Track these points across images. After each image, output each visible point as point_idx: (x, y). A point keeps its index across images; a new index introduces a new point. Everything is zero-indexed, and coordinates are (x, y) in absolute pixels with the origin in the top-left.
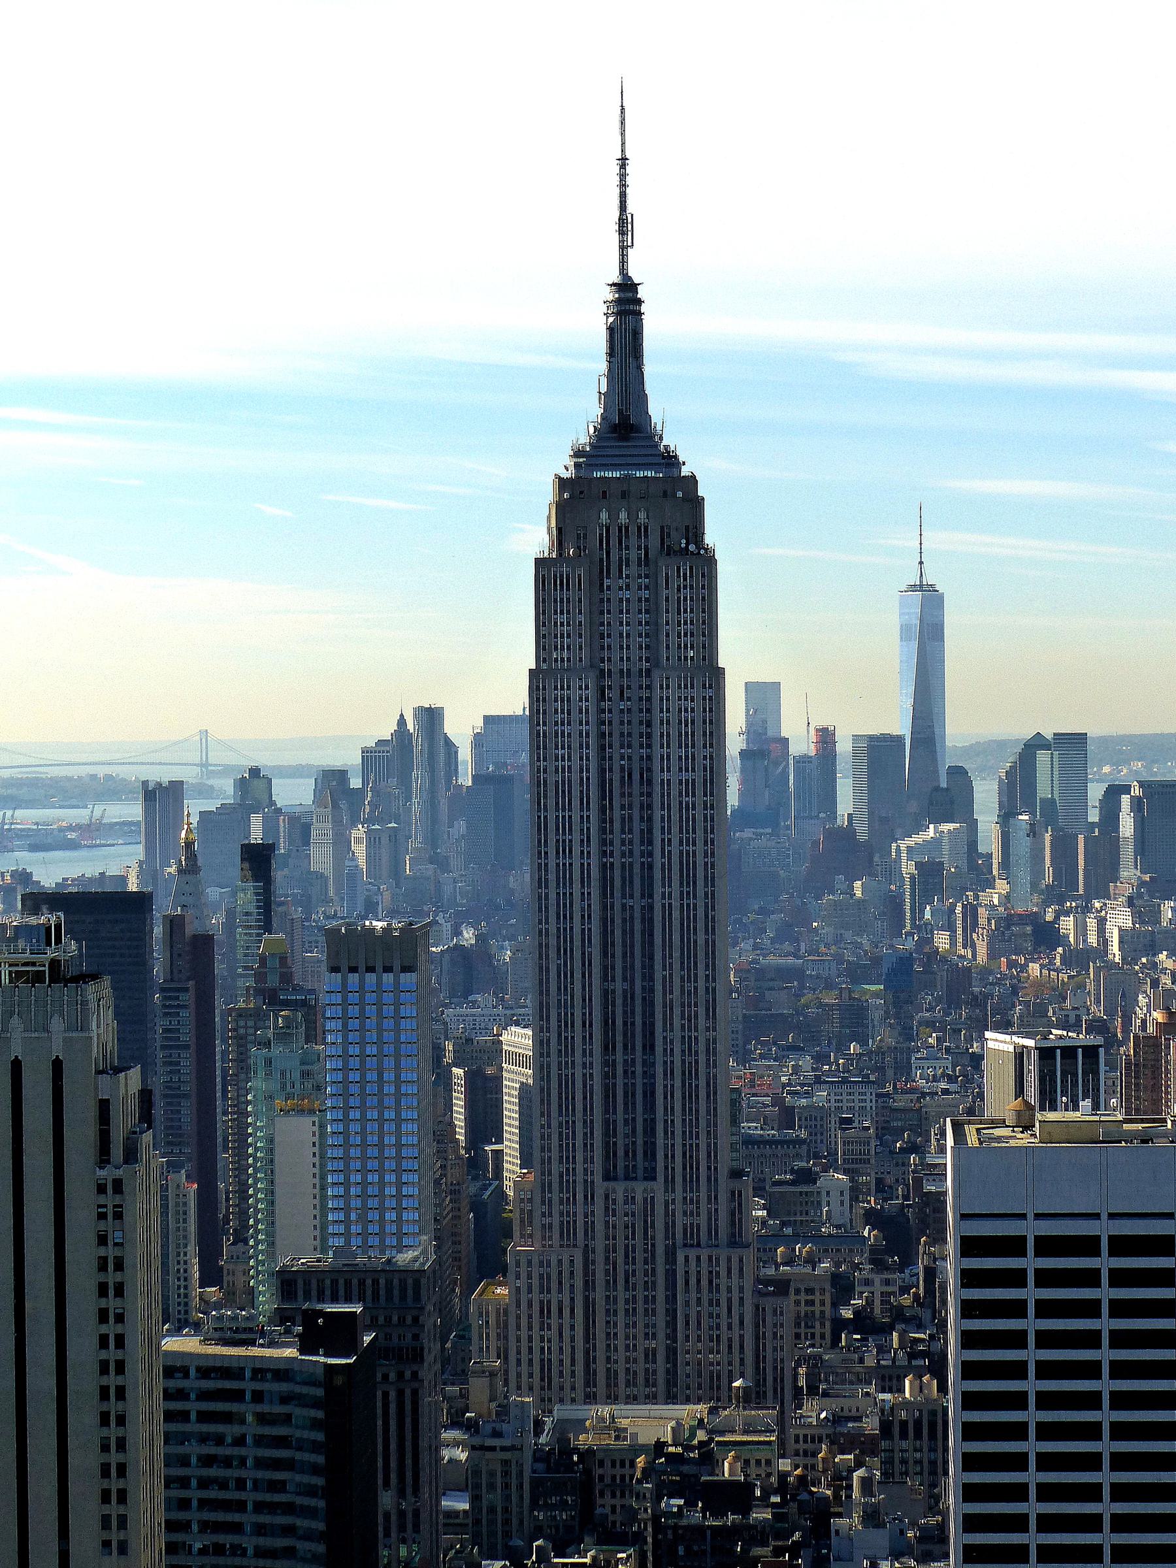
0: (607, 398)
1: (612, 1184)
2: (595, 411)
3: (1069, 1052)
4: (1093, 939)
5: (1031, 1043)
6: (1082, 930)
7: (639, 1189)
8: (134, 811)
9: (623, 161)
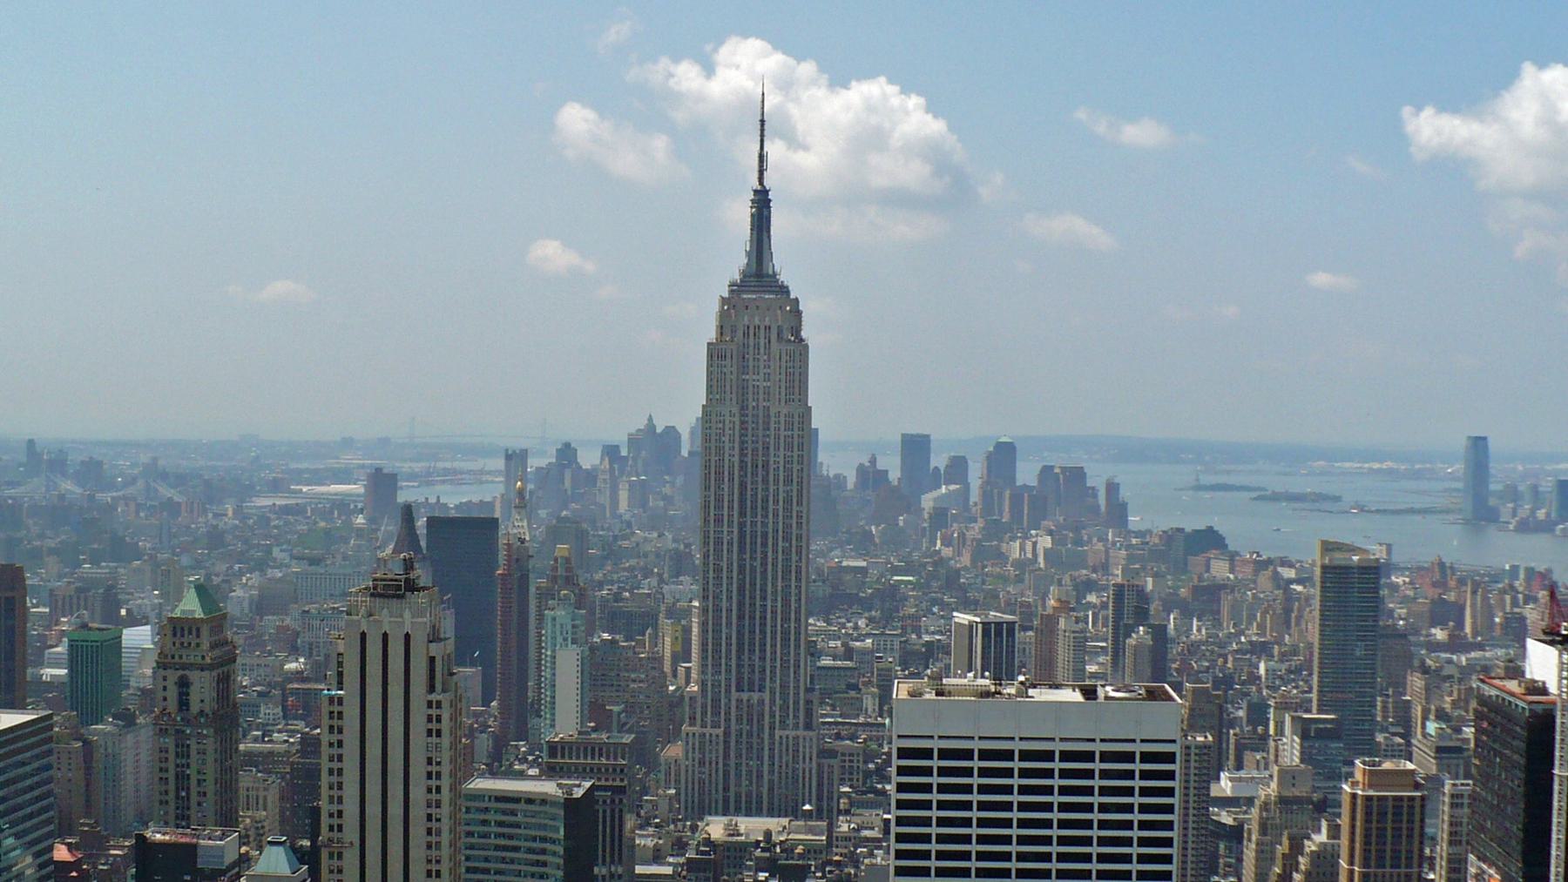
0: (748, 254)
1: (742, 693)
2: (743, 261)
3: (999, 625)
4: (1029, 555)
5: (978, 620)
6: (1022, 549)
7: (756, 696)
8: (500, 464)
9: (762, 122)
